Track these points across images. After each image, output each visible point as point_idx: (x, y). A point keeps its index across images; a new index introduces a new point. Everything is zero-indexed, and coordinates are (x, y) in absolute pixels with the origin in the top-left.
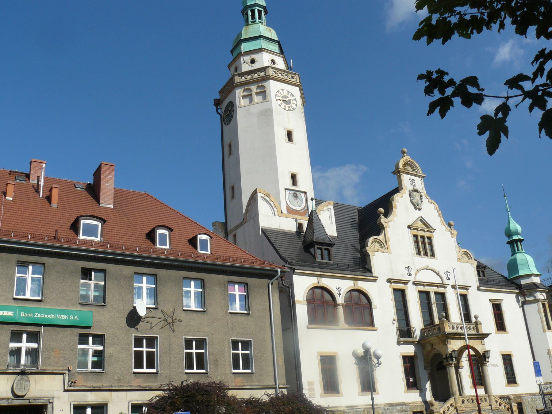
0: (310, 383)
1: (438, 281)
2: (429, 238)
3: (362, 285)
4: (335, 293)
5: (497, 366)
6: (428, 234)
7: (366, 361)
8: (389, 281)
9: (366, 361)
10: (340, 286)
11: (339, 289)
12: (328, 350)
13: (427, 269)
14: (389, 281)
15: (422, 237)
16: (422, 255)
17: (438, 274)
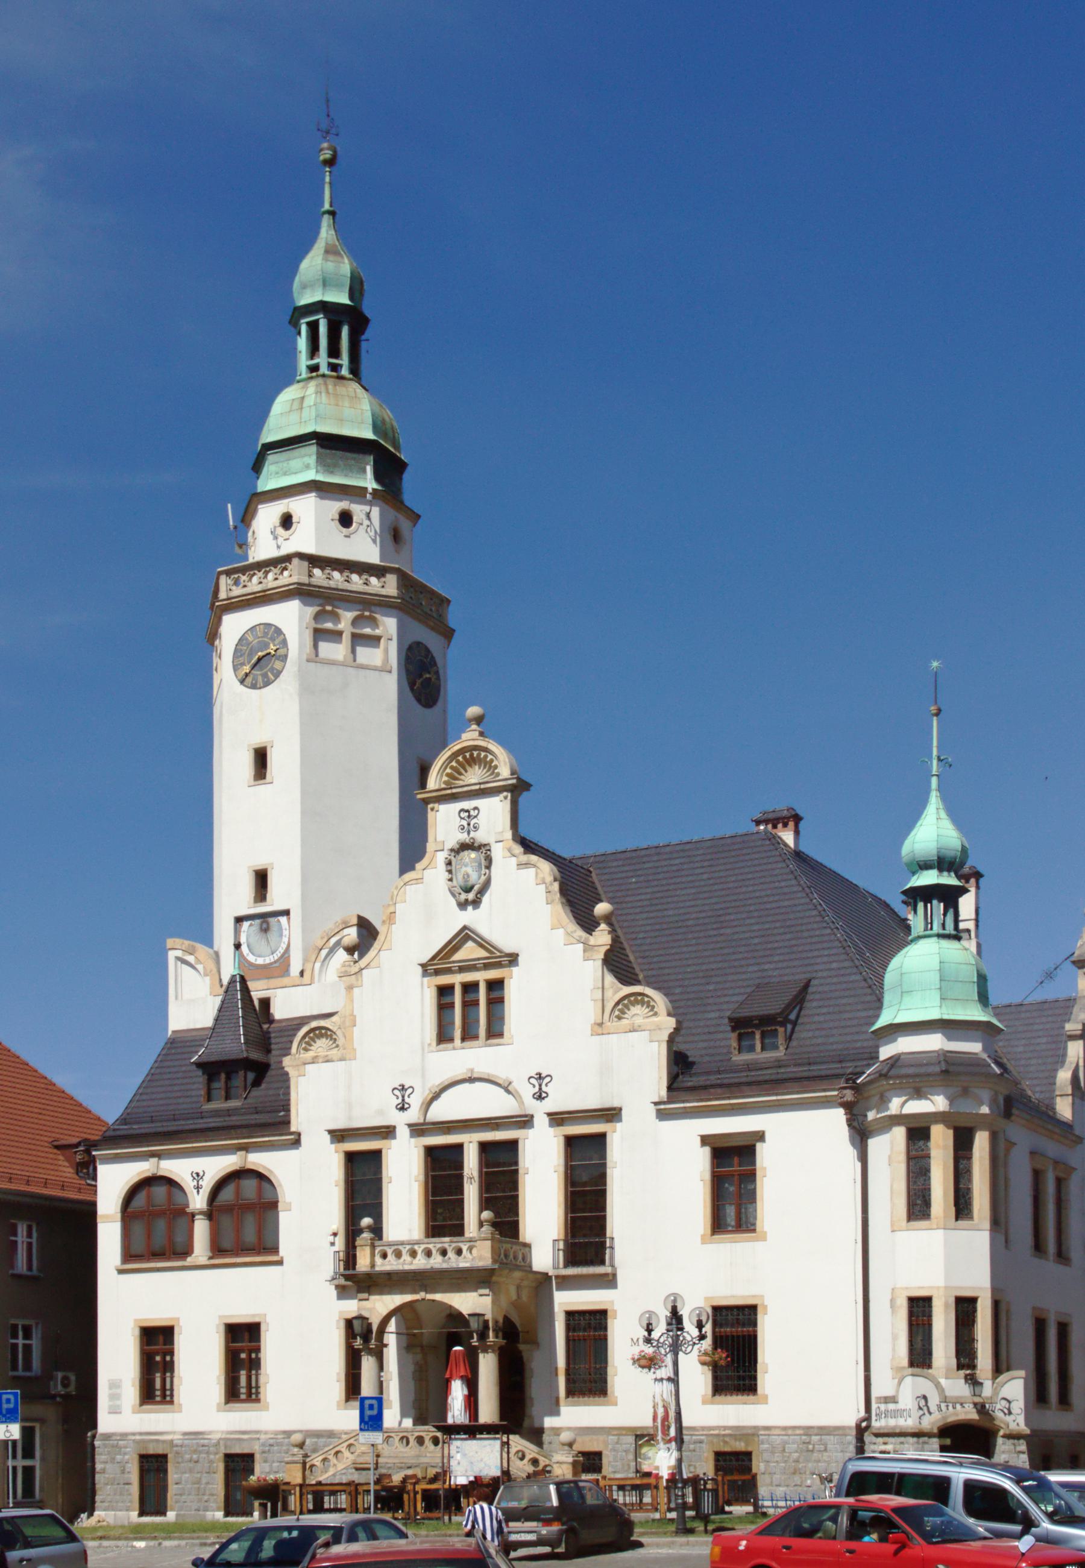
0: (114, 1385)
2: (495, 986)
3: (258, 1160)
4: (188, 1184)
6: (493, 974)
7: (243, 1342)
9: (243, 1342)
10: (197, 1172)
11: (198, 1176)
12: (157, 1317)
14: (338, 1135)
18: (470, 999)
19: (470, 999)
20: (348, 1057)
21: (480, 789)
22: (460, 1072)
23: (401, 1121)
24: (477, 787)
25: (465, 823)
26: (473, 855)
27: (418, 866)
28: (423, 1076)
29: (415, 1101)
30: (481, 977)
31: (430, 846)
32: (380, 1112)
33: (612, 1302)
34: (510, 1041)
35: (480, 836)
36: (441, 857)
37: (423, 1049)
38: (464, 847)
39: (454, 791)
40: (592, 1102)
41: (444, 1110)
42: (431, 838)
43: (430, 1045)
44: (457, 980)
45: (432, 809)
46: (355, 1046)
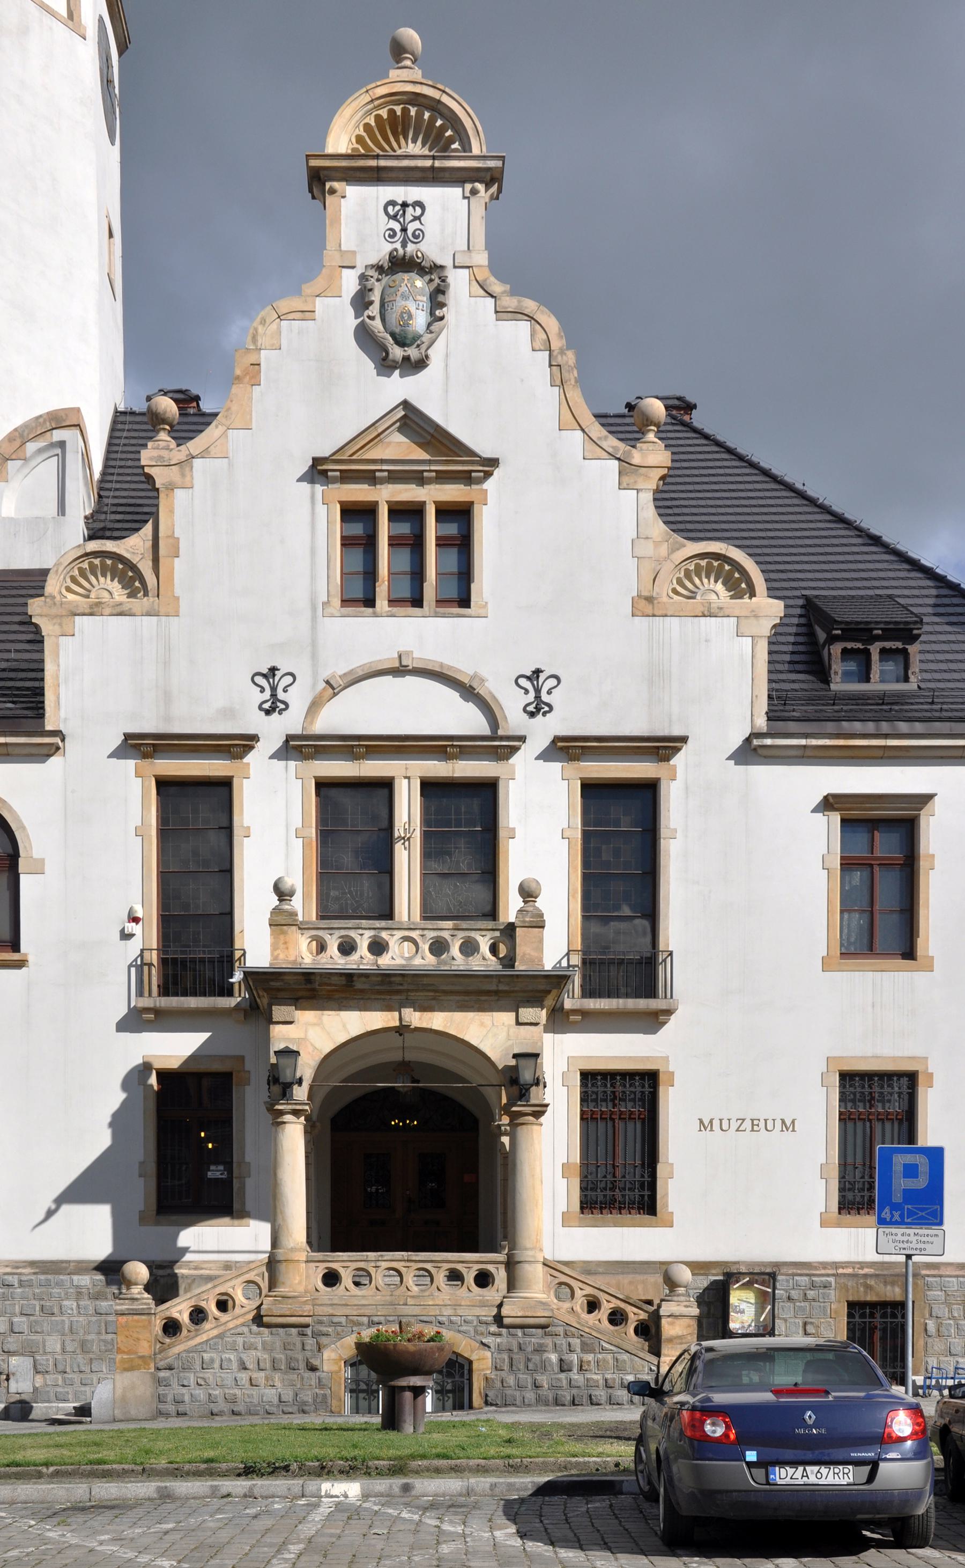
1: (464, 719)
5: (788, 1126)
6: (452, 493)
8: (138, 746)
13: (400, 671)
14: (138, 746)
15: (408, 513)
16: (382, 603)
17: (468, 692)
18: (408, 529)
19: (408, 529)
20: (162, 611)
21: (432, 168)
22: (386, 656)
23: (271, 732)
24: (428, 163)
25: (397, 227)
26: (419, 283)
27: (308, 289)
28: (314, 656)
29: (297, 698)
30: (431, 495)
31: (331, 257)
32: (229, 713)
33: (666, 1059)
34: (482, 612)
35: (431, 248)
36: (350, 283)
37: (314, 609)
38: (400, 264)
39: (383, 163)
40: (635, 725)
41: (351, 715)
42: (330, 245)
43: (326, 604)
44: (385, 495)
45: (333, 191)
46: (178, 592)
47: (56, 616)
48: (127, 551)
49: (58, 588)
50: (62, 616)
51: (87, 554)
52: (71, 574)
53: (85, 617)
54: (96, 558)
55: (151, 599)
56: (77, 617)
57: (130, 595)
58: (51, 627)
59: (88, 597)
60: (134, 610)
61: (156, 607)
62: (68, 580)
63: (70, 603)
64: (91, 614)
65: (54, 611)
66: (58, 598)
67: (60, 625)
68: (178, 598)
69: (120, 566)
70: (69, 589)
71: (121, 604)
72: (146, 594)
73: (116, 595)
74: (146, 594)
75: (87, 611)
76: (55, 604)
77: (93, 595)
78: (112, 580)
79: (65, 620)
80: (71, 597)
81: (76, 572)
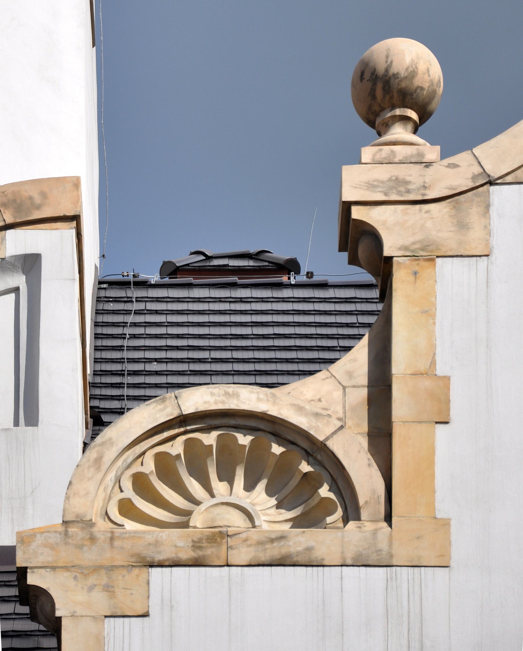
47: (97, 569)
48: (300, 409)
49: (99, 504)
50: (112, 568)
51: (183, 420)
52: (136, 468)
53: (176, 570)
54: (207, 430)
55: (369, 526)
56: (155, 572)
57: (298, 523)
58: (81, 596)
59: (185, 525)
60: (319, 553)
61: (383, 545)
62: (127, 484)
63: (134, 535)
64: (197, 563)
65: (90, 556)
66: (102, 525)
67: (109, 589)
68: (446, 524)
69: (277, 449)
70: (127, 509)
71: (282, 537)
72: (352, 512)
73: (261, 520)
74: (352, 512)
75: (185, 555)
76: (93, 539)
77: (198, 520)
78: (249, 487)
79: (124, 580)
80: (130, 525)
81: (149, 466)
